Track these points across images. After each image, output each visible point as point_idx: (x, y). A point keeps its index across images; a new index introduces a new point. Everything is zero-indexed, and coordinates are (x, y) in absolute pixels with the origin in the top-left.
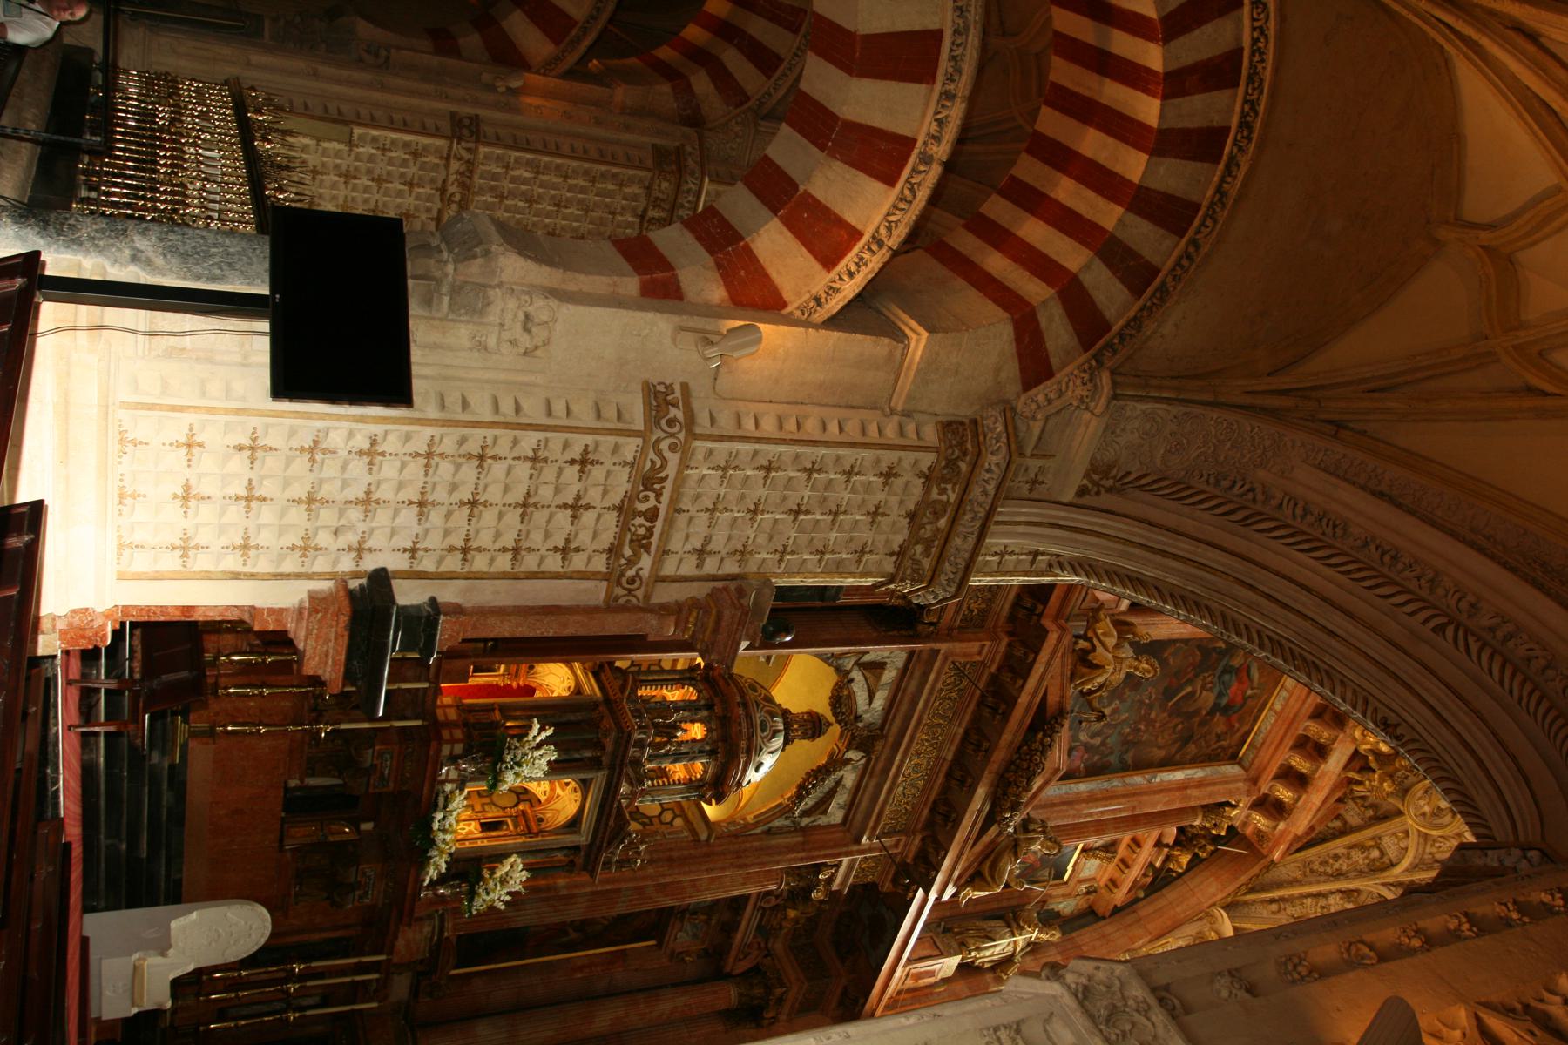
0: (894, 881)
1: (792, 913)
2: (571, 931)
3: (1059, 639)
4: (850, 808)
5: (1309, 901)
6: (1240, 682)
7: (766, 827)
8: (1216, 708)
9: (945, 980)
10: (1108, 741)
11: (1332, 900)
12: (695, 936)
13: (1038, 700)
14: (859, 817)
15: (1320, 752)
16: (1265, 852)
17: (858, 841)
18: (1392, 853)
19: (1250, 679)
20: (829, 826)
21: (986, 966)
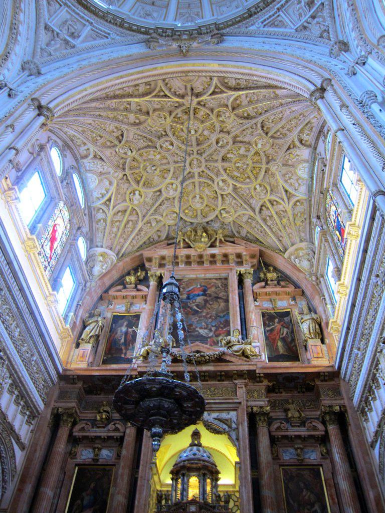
0: (261, 382)
1: (290, 415)
2: (313, 509)
3: (140, 367)
4: (228, 410)
5: (274, 230)
6: (194, 291)
8: (205, 295)
9: (323, 342)
10: (214, 325)
11: (269, 224)
12: (313, 451)
15: (213, 256)
16: (258, 254)
17: (240, 403)
18: (247, 217)
20: (237, 416)
21: (317, 326)
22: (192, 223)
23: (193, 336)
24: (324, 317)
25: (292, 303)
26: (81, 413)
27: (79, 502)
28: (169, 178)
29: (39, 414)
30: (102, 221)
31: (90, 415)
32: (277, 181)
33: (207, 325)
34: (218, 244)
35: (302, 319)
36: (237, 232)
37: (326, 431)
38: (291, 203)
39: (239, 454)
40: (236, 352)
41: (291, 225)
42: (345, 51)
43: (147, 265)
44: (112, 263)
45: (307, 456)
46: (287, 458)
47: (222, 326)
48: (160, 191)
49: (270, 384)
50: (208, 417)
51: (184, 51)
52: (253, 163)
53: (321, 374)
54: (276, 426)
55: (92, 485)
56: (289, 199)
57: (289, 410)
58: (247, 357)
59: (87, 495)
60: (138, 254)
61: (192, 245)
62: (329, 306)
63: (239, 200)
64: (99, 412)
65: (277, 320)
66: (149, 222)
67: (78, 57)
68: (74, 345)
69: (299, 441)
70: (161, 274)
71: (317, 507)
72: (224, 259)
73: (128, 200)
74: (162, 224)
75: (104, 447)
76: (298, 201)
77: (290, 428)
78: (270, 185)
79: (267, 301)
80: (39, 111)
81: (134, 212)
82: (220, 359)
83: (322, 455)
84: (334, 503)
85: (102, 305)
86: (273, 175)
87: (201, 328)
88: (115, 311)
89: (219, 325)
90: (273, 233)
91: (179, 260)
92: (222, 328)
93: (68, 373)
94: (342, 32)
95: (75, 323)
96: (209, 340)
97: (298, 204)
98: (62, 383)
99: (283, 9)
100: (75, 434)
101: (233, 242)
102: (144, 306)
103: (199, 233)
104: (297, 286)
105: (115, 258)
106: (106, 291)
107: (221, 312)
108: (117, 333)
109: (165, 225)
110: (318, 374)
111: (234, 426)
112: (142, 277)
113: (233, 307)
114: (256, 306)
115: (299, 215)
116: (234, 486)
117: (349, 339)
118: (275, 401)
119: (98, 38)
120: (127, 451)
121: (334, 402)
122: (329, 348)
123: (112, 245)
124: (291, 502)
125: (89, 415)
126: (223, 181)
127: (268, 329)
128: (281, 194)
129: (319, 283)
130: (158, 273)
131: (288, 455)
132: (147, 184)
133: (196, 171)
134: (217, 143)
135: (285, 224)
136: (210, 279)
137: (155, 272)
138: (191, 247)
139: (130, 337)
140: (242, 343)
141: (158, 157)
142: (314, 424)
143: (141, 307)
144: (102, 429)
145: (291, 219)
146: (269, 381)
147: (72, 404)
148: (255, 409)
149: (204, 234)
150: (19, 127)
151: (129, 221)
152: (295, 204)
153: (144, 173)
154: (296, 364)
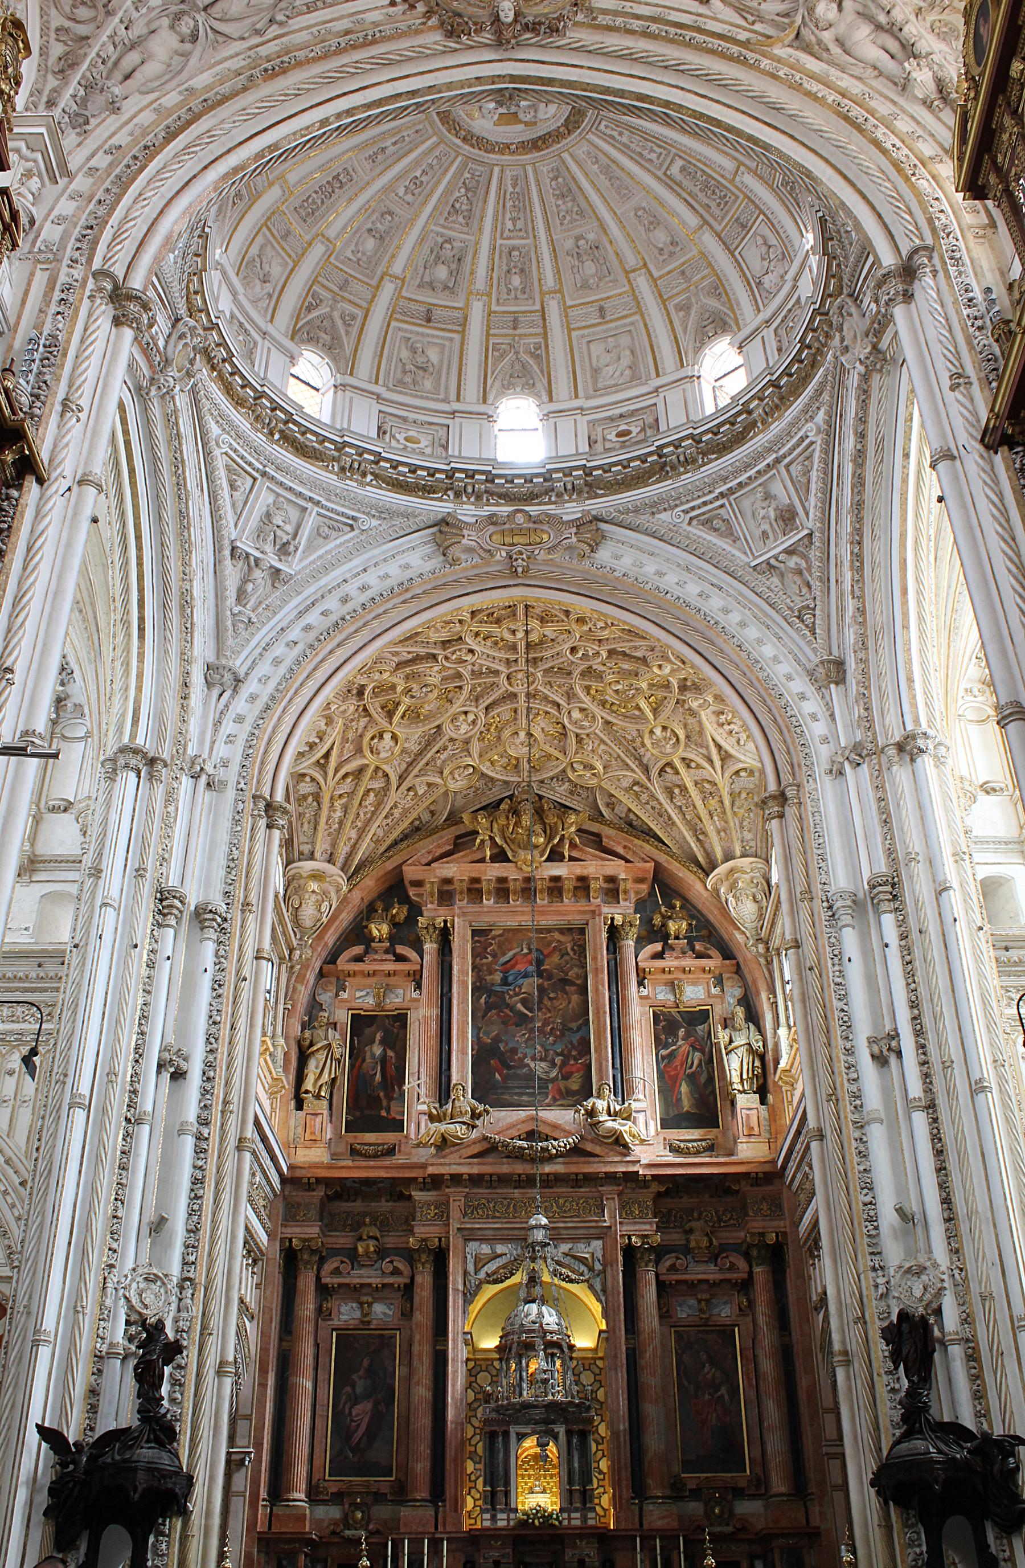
0: (648, 1187)
1: (693, 1244)
4: (588, 1239)
5: (688, 817)
6: (516, 963)
7: (601, 1294)
8: (540, 974)
9: (763, 1101)
12: (725, 1303)
13: (475, 1160)
14: (593, 1231)
15: (556, 879)
17: (610, 1227)
19: (515, 955)
21: (757, 1063)
22: (506, 783)
23: (520, 1077)
24: (770, 1045)
25: (713, 991)
26: (325, 1236)
27: (348, 1389)
28: (459, 702)
29: (263, 1254)
30: (310, 799)
31: (342, 1241)
32: (700, 722)
33: (546, 1051)
34: (566, 854)
35: (731, 1041)
36: (608, 805)
37: (751, 1273)
38: (727, 775)
39: (605, 1314)
40: (604, 1137)
41: (724, 812)
42: (837, 684)
43: (412, 892)
44: (338, 891)
45: (715, 1311)
46: (684, 1315)
47: (574, 1053)
48: (439, 727)
49: (662, 1189)
50: (554, 1251)
51: (520, 570)
52: (651, 686)
53: (753, 1175)
54: (668, 1264)
55: (366, 1363)
56: (722, 760)
57: (691, 1231)
58: (626, 1146)
59: (360, 1378)
60: (390, 865)
61: (510, 855)
62: (782, 1032)
63: (616, 748)
64: (360, 1239)
65: (681, 1032)
66: (409, 790)
67: (300, 598)
68: (293, 1103)
69: (705, 1287)
70: (445, 922)
71: (723, 1391)
72: (579, 884)
73: (368, 753)
74: (442, 790)
75: (376, 1300)
76: (745, 769)
77: (693, 1268)
78: (685, 726)
79: (666, 984)
80: (268, 817)
81: (380, 774)
82: (576, 1151)
83: (740, 1309)
84: (750, 1385)
85: (325, 991)
86: (693, 713)
87: (533, 1059)
88: (354, 1005)
89: (570, 1051)
90: (688, 823)
91: (484, 885)
92: (576, 1059)
93: (299, 1173)
94: (838, 625)
95: (285, 1054)
96: (550, 1086)
97: (743, 774)
98: (288, 1188)
99: (732, 498)
100: (324, 1280)
101: (597, 841)
102: (414, 995)
103: (526, 820)
104: (727, 953)
105: (342, 880)
106: (332, 959)
107: (573, 1020)
108: (364, 1060)
109: (446, 793)
110: (746, 1175)
111: (598, 1267)
112: (402, 917)
113: (598, 1013)
114: (641, 997)
115: (744, 795)
116: (595, 1350)
117: (798, 1146)
118: (669, 1211)
119: (334, 534)
120: (423, 1316)
121: (767, 1224)
122: (774, 1115)
123: (334, 845)
124: (686, 1383)
125: (342, 1240)
126: (582, 710)
127: (663, 1052)
128: (707, 748)
129: (769, 963)
130: (439, 922)
131: (685, 1310)
132: (414, 716)
133: (520, 689)
134: (573, 650)
135: (712, 808)
136: (549, 931)
137: (434, 918)
138: (509, 861)
139: (392, 1070)
140: (616, 1114)
141: (436, 669)
142: (731, 1259)
143: (408, 998)
144: (371, 1272)
145: (727, 803)
146: (660, 1183)
147: (313, 1230)
148: (634, 1239)
149: (538, 828)
150: (253, 898)
151: (369, 791)
152: (737, 773)
153: (407, 700)
154: (712, 1133)
